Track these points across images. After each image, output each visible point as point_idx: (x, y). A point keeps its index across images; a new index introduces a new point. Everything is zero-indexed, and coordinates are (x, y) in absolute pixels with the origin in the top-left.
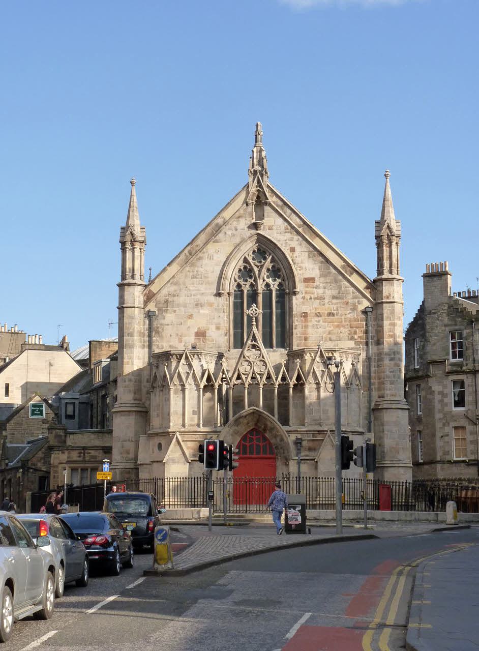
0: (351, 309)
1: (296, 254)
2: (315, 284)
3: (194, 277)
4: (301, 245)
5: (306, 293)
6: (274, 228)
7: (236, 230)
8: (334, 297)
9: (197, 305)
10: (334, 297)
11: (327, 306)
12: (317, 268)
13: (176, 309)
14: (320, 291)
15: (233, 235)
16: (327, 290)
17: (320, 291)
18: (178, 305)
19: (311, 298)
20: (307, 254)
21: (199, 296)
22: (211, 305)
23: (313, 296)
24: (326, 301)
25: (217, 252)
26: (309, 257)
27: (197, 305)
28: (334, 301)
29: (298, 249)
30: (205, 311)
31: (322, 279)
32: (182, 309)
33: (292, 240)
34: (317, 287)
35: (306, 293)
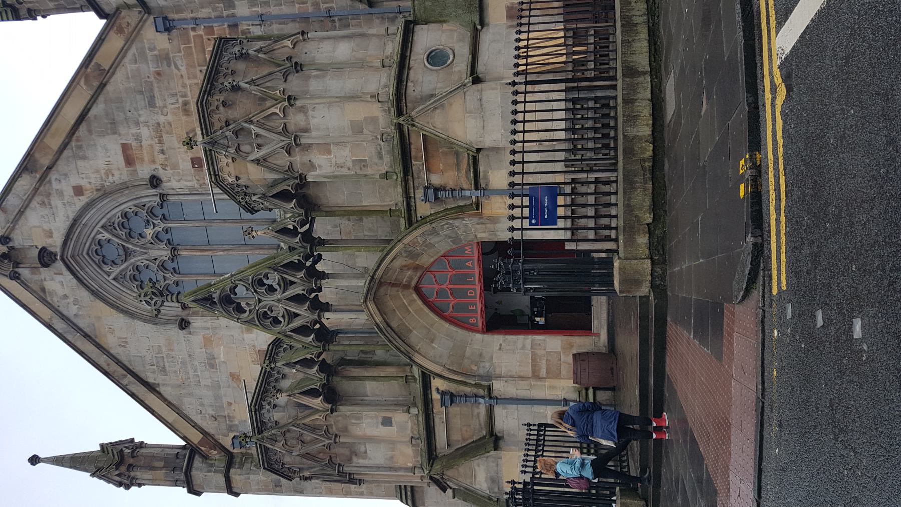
0: (169, 65)
1: (83, 183)
2: (134, 144)
3: (164, 371)
4: (66, 175)
5: (154, 162)
6: (46, 226)
7: (65, 297)
8: (152, 104)
9: (212, 366)
10: (152, 104)
11: (170, 117)
12: (101, 141)
13: (225, 401)
14: (145, 132)
15: (76, 302)
16: (142, 119)
17: (145, 132)
18: (217, 398)
19: (162, 152)
20: (81, 163)
21: (196, 363)
22: (208, 342)
23: (157, 147)
24: (162, 119)
25: (111, 331)
26: (84, 158)
27: (212, 366)
28: (159, 103)
29: (74, 180)
30: (221, 353)
31: (122, 129)
32: (222, 392)
33: (60, 193)
34: (138, 138)
35: (154, 162)
